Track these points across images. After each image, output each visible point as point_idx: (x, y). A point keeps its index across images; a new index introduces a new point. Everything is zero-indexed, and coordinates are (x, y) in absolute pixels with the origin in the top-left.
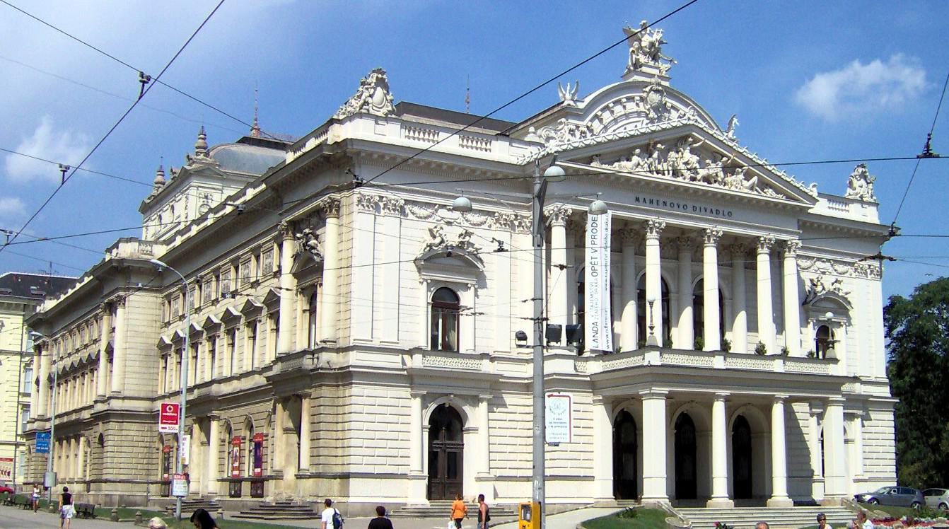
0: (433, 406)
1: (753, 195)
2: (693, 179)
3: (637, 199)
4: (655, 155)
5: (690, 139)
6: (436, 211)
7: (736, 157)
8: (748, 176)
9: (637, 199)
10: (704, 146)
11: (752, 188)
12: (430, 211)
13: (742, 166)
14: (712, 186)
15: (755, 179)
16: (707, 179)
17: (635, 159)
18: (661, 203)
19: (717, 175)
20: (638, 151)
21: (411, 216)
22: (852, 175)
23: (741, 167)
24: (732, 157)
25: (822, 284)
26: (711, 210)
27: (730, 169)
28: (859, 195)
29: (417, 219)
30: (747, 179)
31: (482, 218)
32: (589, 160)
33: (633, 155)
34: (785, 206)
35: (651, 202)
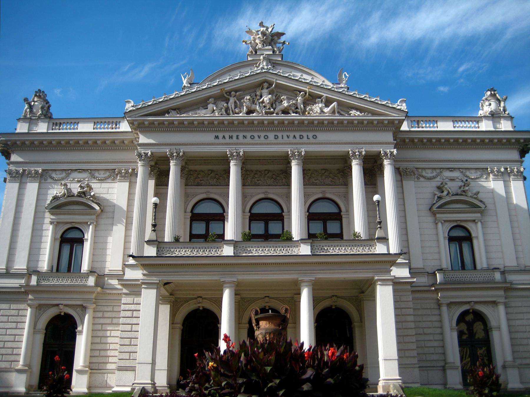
0: (51, 313)
1: (337, 117)
2: (273, 113)
3: (217, 137)
4: (232, 100)
5: (266, 85)
6: (70, 174)
7: (310, 89)
8: (328, 102)
9: (217, 137)
10: (278, 86)
11: (333, 112)
12: (64, 175)
13: (321, 96)
14: (289, 115)
15: (335, 104)
16: (285, 112)
17: (210, 106)
18: (241, 137)
19: (297, 108)
20: (210, 100)
21: (50, 180)
22: (483, 99)
23: (320, 97)
24: (307, 90)
25: (446, 188)
26: (294, 137)
27: (311, 99)
28: (488, 112)
29: (54, 181)
30: (327, 106)
31: (108, 174)
32: (167, 112)
33: (209, 104)
34: (371, 122)
35: (231, 137)
